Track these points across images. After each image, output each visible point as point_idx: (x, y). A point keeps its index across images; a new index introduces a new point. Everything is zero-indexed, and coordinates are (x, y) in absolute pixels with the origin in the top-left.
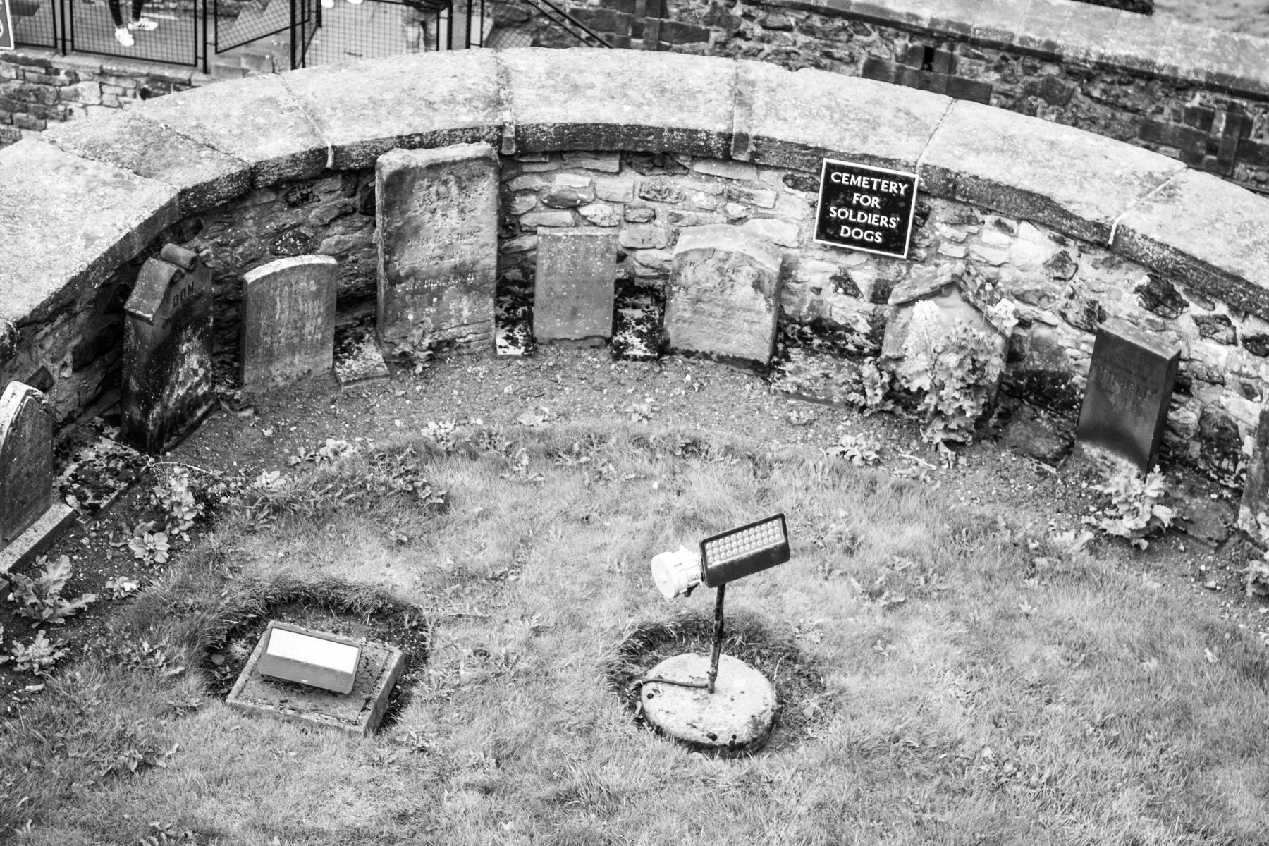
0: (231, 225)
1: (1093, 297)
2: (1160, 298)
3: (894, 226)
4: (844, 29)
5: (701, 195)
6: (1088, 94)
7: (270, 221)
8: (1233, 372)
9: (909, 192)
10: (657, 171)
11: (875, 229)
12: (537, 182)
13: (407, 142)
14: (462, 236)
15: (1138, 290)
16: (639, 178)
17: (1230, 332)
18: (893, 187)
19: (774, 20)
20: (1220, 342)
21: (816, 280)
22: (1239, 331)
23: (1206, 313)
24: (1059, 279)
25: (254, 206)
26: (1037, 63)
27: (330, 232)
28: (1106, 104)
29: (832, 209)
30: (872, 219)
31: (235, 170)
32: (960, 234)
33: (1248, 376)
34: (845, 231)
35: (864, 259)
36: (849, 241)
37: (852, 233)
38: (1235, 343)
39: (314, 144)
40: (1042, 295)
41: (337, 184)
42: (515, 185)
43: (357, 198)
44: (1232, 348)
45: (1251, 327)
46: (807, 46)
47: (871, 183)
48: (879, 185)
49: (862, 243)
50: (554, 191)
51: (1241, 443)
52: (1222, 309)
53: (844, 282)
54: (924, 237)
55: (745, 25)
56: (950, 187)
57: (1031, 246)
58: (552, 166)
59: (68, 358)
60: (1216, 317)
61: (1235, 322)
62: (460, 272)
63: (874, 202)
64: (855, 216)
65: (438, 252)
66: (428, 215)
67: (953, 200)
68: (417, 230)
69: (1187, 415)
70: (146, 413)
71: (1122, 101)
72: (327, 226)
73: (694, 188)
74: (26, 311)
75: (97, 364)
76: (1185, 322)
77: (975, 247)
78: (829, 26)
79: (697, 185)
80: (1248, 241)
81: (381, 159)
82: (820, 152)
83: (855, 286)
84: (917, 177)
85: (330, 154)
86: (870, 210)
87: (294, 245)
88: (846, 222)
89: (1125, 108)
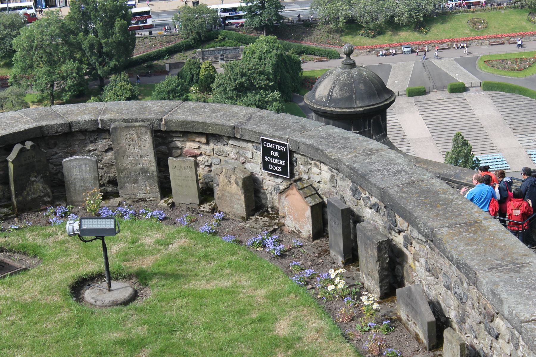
0: (70, 146)
1: (342, 193)
3: (284, 164)
5: (233, 154)
16: (215, 147)
24: (333, 187)
25: (78, 140)
27: (107, 154)
29: (266, 157)
30: (277, 161)
37: (272, 167)
47: (275, 147)
68: (125, 152)
73: (229, 149)
77: (311, 175)
82: (260, 134)
84: (288, 144)
88: (270, 163)
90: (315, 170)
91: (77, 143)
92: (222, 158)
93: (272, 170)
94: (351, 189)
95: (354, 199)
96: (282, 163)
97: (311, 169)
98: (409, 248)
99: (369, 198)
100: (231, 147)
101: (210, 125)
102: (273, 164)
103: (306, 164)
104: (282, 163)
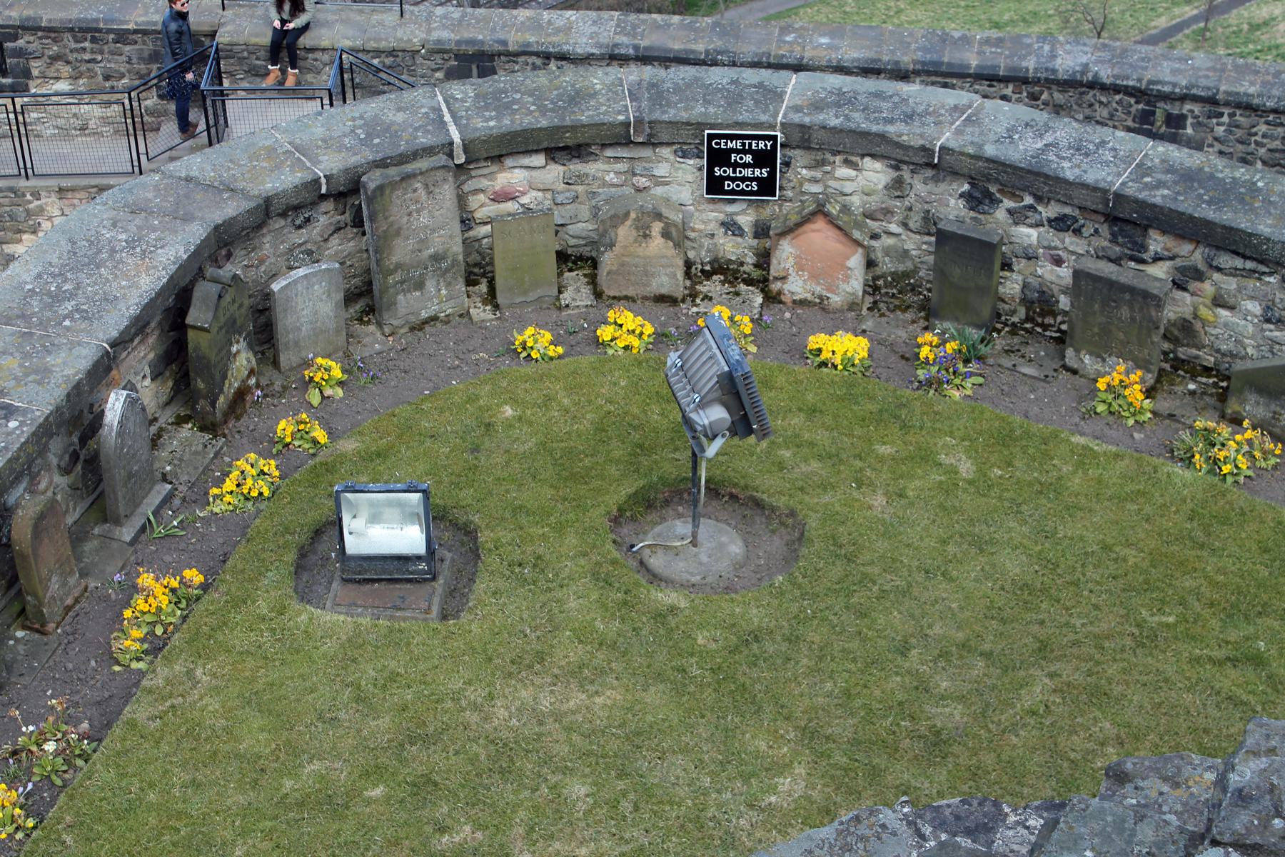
0: (253, 250)
1: (926, 207)
2: (979, 199)
5: (612, 175)
7: (283, 242)
8: (1044, 247)
9: (774, 146)
10: (576, 161)
11: (751, 180)
12: (484, 183)
13: (382, 164)
14: (433, 231)
15: (961, 196)
16: (561, 168)
17: (1038, 217)
18: (761, 145)
20: (1031, 226)
21: (712, 227)
22: (1044, 214)
23: (1016, 205)
25: (269, 232)
27: (330, 245)
29: (716, 169)
30: (748, 172)
31: (252, 204)
32: (819, 175)
33: (1055, 248)
34: (728, 185)
35: (744, 206)
36: (733, 192)
37: (733, 186)
38: (1043, 225)
39: (310, 177)
40: (888, 212)
41: (328, 205)
42: (466, 188)
43: (347, 214)
44: (1041, 229)
47: (744, 144)
48: (750, 145)
49: (743, 192)
50: (497, 188)
51: (1058, 302)
52: (1028, 200)
53: (731, 227)
54: (790, 181)
56: (802, 138)
57: (875, 174)
58: (494, 168)
59: (147, 370)
60: (1025, 207)
61: (1040, 208)
62: (437, 258)
63: (748, 158)
64: (734, 172)
65: (416, 247)
66: (406, 218)
67: (809, 148)
69: (1011, 286)
70: (213, 404)
72: (326, 240)
73: (604, 171)
74: (115, 334)
75: (167, 374)
76: (1001, 214)
77: (831, 183)
79: (606, 167)
80: (1040, 145)
81: (364, 179)
82: (701, 126)
83: (740, 228)
84: (779, 134)
85: (323, 181)
86: (745, 166)
87: (304, 260)
88: (729, 178)
92: (580, 188)
93: (733, 192)
95: (972, 214)
99: (1036, 210)
100: (609, 163)
101: (566, 129)
102: (733, 180)
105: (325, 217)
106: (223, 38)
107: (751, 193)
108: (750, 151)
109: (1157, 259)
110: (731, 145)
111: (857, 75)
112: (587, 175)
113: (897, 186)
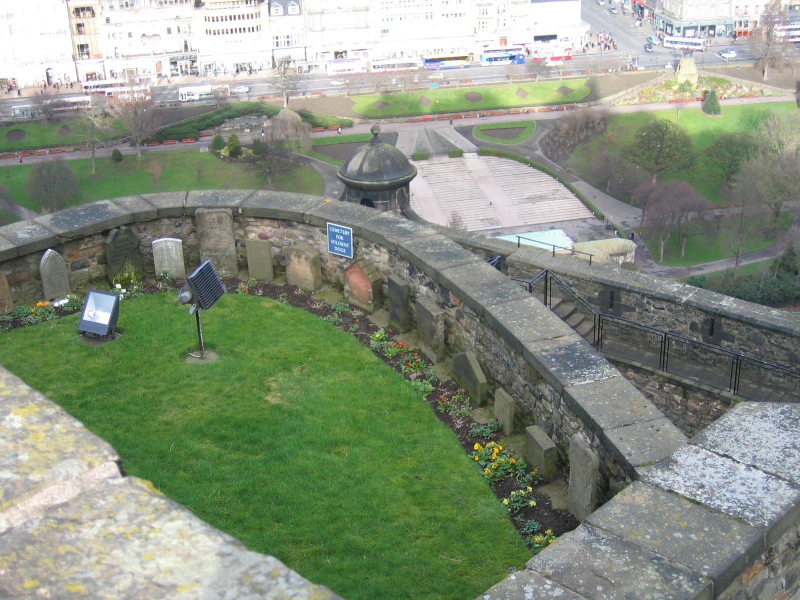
0: (158, 230)
2: (412, 271)
4: (682, 310)
6: (769, 341)
12: (255, 229)
19: (658, 305)
26: (751, 327)
28: (777, 346)
30: (342, 244)
36: (337, 252)
45: (428, 280)
46: (670, 316)
55: (647, 307)
58: (259, 224)
71: (782, 345)
72: (189, 234)
73: (298, 232)
77: (372, 256)
78: (677, 309)
86: (341, 241)
88: (336, 245)
89: (783, 348)
90: (375, 252)
91: (164, 227)
94: (408, 268)
96: (347, 246)
97: (371, 251)
98: (461, 320)
101: (283, 212)
103: (368, 246)
104: (347, 246)
105: (187, 227)
106: (512, 257)
107: (343, 253)
108: (342, 235)
109: (453, 306)
110: (337, 230)
111: (429, 223)
112: (293, 234)
113: (390, 260)
